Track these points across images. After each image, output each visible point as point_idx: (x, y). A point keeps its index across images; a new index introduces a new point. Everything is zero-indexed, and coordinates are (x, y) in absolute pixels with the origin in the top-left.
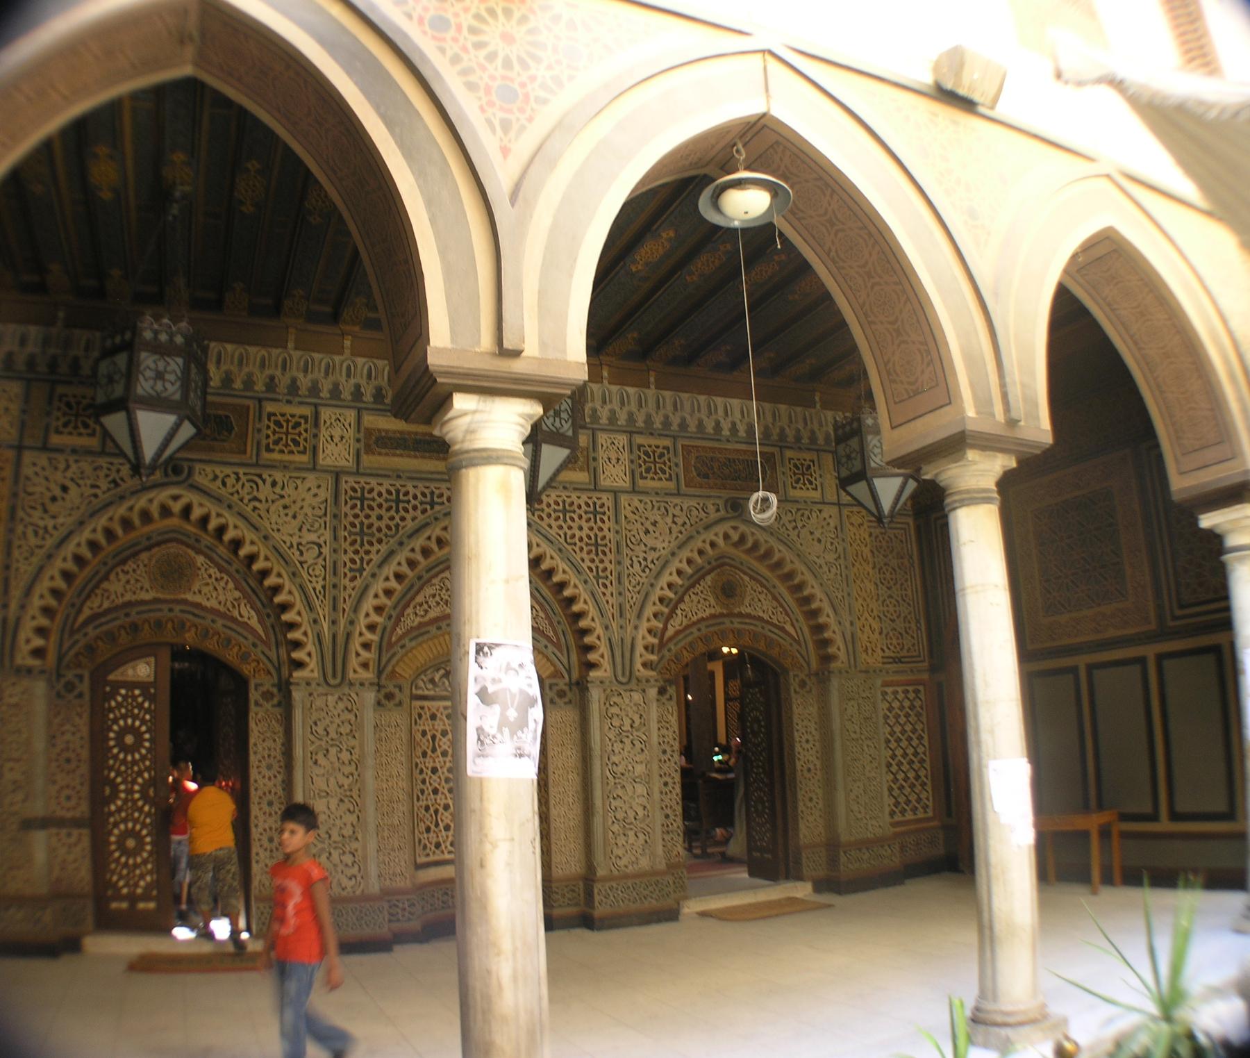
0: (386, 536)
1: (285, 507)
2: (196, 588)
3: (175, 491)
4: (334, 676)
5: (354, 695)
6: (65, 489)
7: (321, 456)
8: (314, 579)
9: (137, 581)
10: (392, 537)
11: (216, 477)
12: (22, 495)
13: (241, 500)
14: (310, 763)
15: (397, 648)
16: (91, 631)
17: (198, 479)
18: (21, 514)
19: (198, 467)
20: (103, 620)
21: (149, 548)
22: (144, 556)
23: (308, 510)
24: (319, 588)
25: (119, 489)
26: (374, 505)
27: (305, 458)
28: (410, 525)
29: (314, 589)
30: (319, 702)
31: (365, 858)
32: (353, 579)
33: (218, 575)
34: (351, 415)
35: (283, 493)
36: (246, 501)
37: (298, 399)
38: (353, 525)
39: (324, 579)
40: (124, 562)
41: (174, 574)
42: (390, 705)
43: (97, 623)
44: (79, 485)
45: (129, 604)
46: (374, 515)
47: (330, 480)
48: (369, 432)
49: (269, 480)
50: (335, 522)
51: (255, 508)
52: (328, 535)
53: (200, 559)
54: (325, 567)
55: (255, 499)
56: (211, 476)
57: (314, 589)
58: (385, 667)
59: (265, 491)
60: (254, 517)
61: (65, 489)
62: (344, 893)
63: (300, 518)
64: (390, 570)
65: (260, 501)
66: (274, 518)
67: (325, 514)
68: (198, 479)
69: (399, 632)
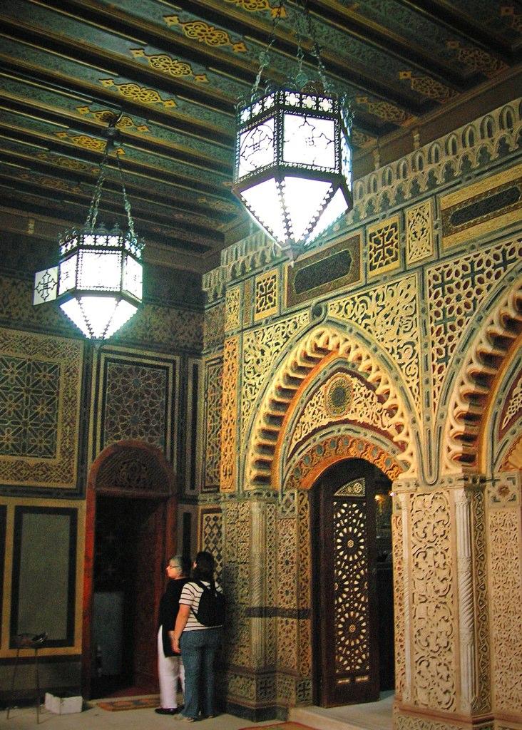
0: (466, 315)
1: (386, 316)
2: (353, 405)
3: (317, 330)
4: (431, 474)
5: (445, 492)
6: (263, 352)
7: (408, 256)
8: (410, 379)
9: (319, 411)
10: (471, 315)
11: (341, 307)
12: (244, 365)
13: (357, 321)
14: (413, 566)
15: (508, 436)
16: (297, 458)
17: (332, 314)
18: (244, 379)
19: (330, 303)
20: (303, 447)
21: (324, 383)
22: (322, 389)
23: (402, 313)
24: (415, 387)
25: (290, 340)
26: (453, 285)
27: (396, 264)
28: (486, 296)
29: (411, 388)
30: (418, 504)
31: (458, 671)
32: (440, 372)
33: (367, 392)
34: (428, 204)
35: (383, 303)
36: (360, 321)
37: (390, 211)
38: (437, 314)
39: (418, 377)
40: (311, 398)
41: (340, 397)
42: (504, 500)
43: (299, 450)
44: (269, 347)
45: (315, 431)
46: (453, 296)
47: (417, 274)
48: (446, 212)
49: (374, 297)
50: (424, 317)
51: (366, 325)
52: (418, 330)
53: (355, 381)
54: (417, 364)
55: (366, 317)
56: (338, 308)
57: (411, 388)
58: (497, 460)
59: (373, 306)
60: (367, 335)
61: (263, 352)
62: (439, 708)
63: (397, 322)
64: (471, 352)
65: (369, 317)
66: (379, 329)
67: (415, 312)
68: (332, 314)
69: (509, 416)
